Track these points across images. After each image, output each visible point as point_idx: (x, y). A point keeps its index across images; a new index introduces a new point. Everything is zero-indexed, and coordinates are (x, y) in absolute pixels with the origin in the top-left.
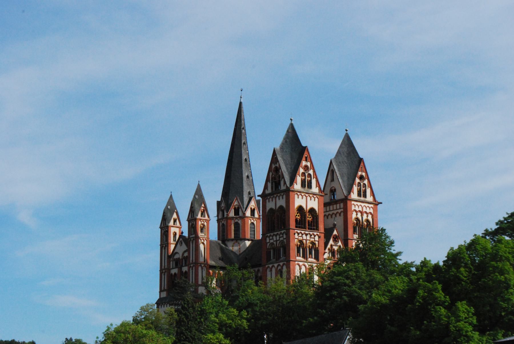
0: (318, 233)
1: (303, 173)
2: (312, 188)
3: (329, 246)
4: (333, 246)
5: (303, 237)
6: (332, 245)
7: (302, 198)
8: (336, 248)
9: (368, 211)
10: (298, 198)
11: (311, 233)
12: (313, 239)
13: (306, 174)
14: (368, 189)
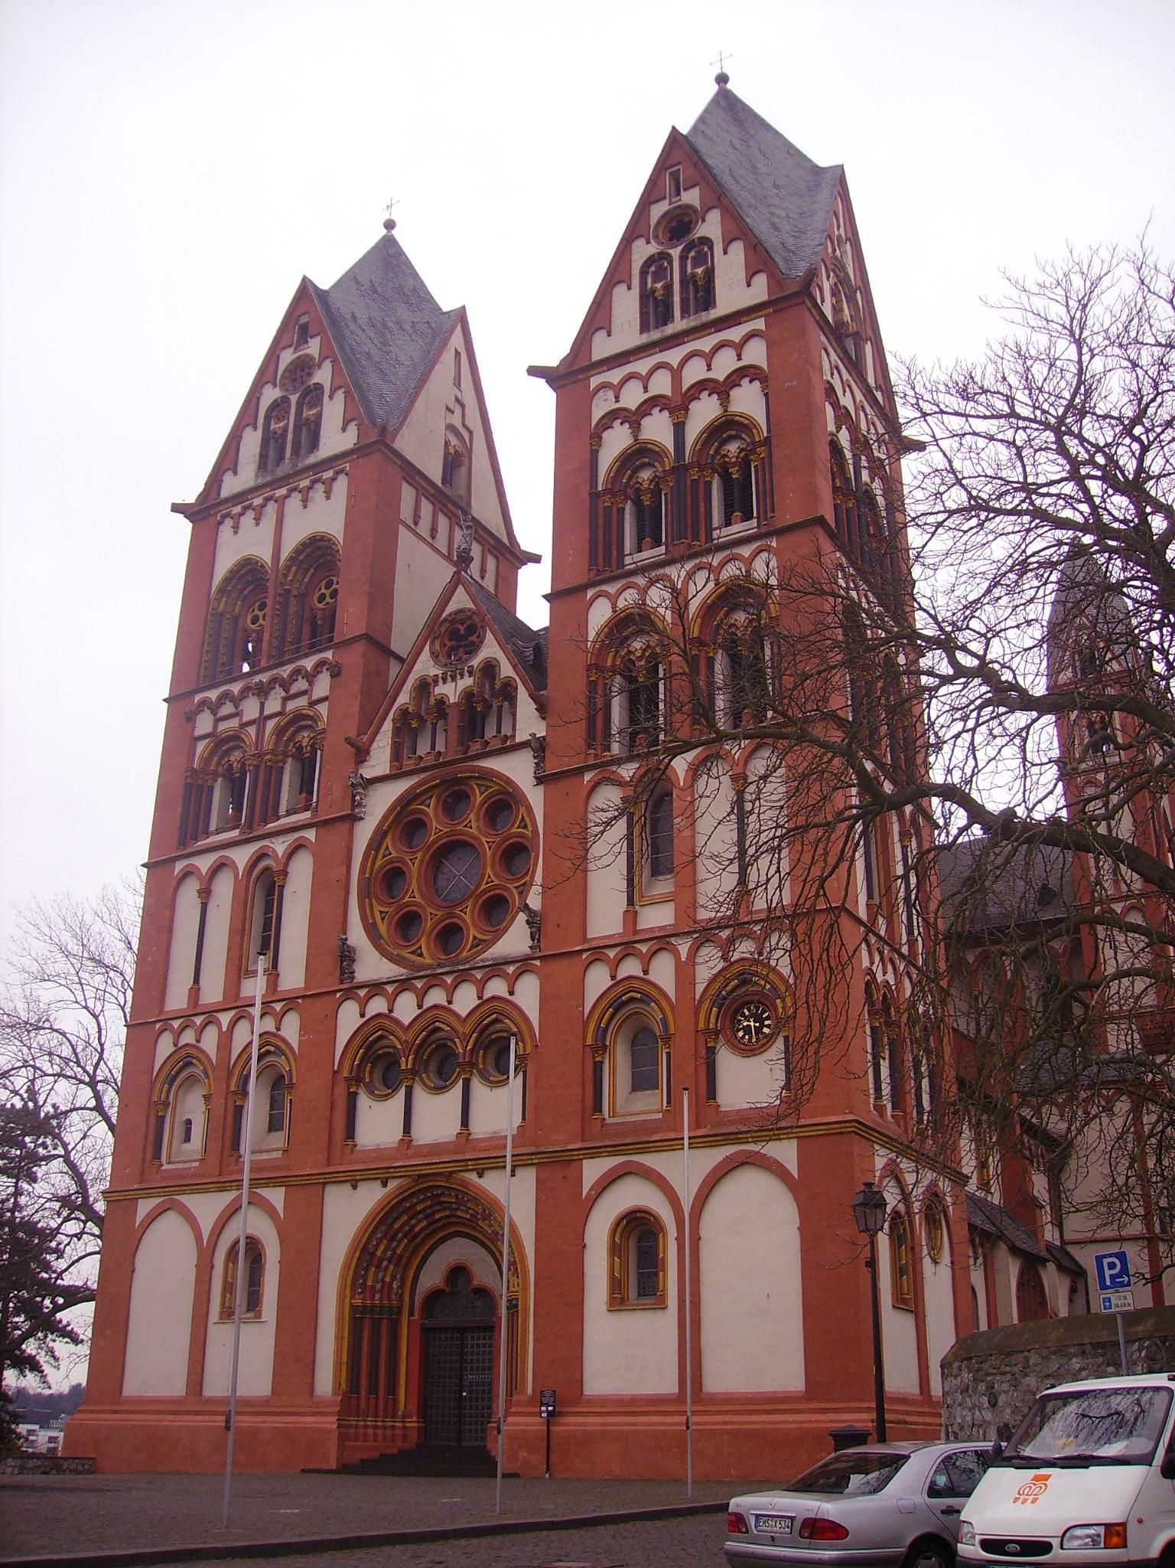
0: (329, 655)
1: (275, 405)
2: (321, 445)
3: (404, 698)
4: (436, 682)
5: (237, 714)
6: (430, 680)
7: (257, 520)
8: (451, 691)
9: (725, 364)
10: (236, 528)
11: (285, 671)
12: (302, 701)
13: (291, 397)
14: (725, 253)
